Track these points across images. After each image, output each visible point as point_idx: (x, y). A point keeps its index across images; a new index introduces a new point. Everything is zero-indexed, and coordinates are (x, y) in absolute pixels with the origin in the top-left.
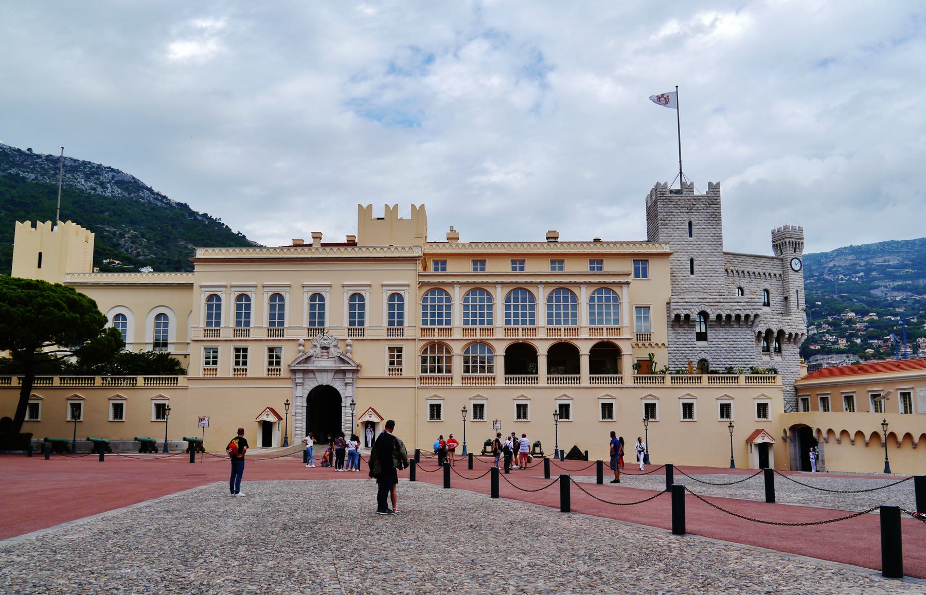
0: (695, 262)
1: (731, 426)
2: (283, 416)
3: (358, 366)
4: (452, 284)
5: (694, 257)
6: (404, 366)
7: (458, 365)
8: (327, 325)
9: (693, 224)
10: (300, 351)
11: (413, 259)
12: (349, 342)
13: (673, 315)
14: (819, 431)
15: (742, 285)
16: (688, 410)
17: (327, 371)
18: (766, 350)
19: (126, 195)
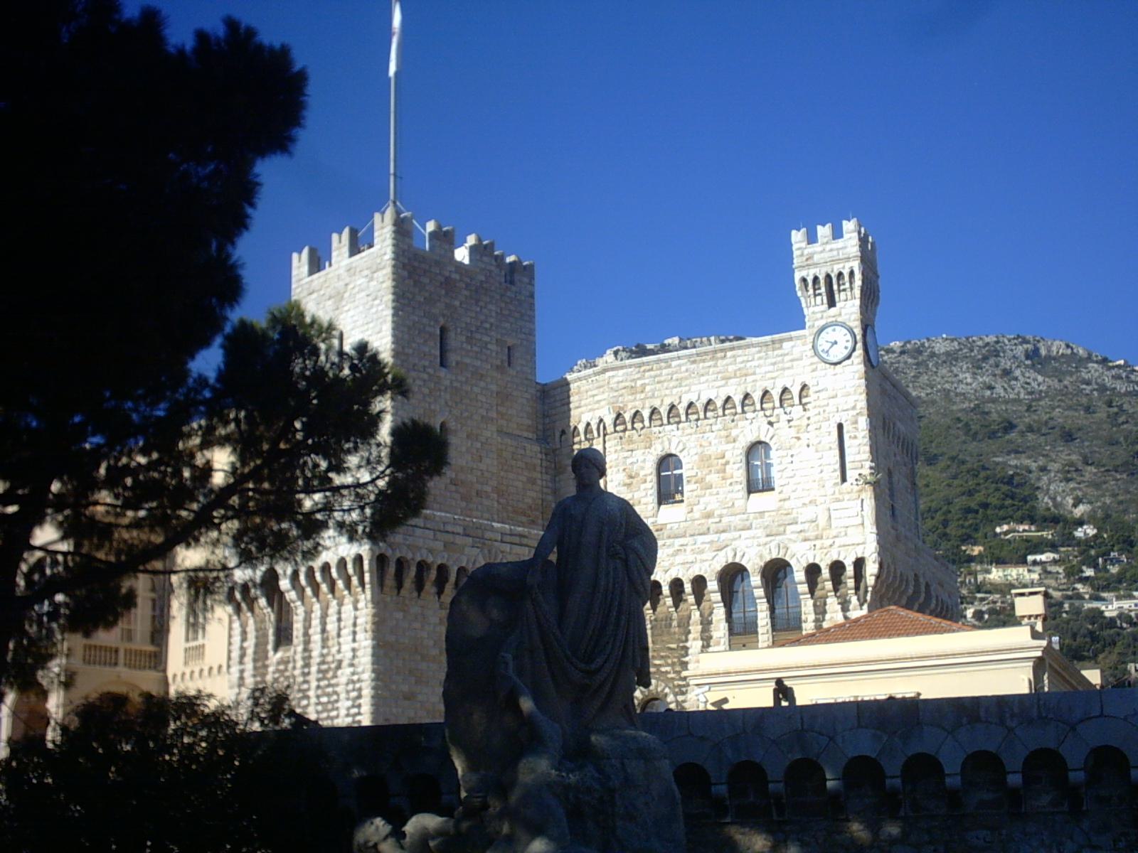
18: (741, 633)
19: (1055, 384)
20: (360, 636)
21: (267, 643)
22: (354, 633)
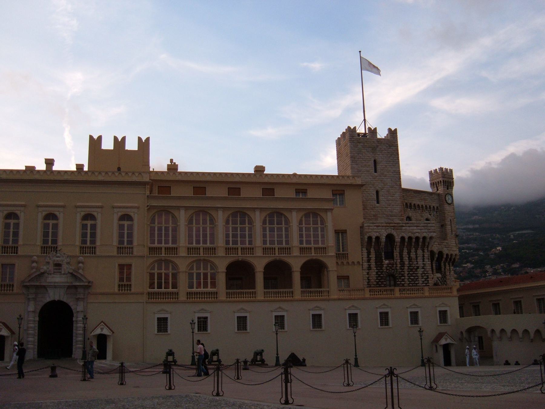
0: (381, 193)
1: (420, 331)
2: (16, 330)
3: (89, 282)
4: (178, 208)
5: (379, 189)
6: (133, 282)
7: (183, 280)
8: (60, 243)
9: (378, 160)
10: (33, 268)
11: (144, 184)
12: (81, 258)
13: (366, 237)
14: (493, 331)
15: (410, 215)
16: (384, 318)
17: (60, 287)
20: (426, 260)
21: (382, 257)
22: (423, 259)
